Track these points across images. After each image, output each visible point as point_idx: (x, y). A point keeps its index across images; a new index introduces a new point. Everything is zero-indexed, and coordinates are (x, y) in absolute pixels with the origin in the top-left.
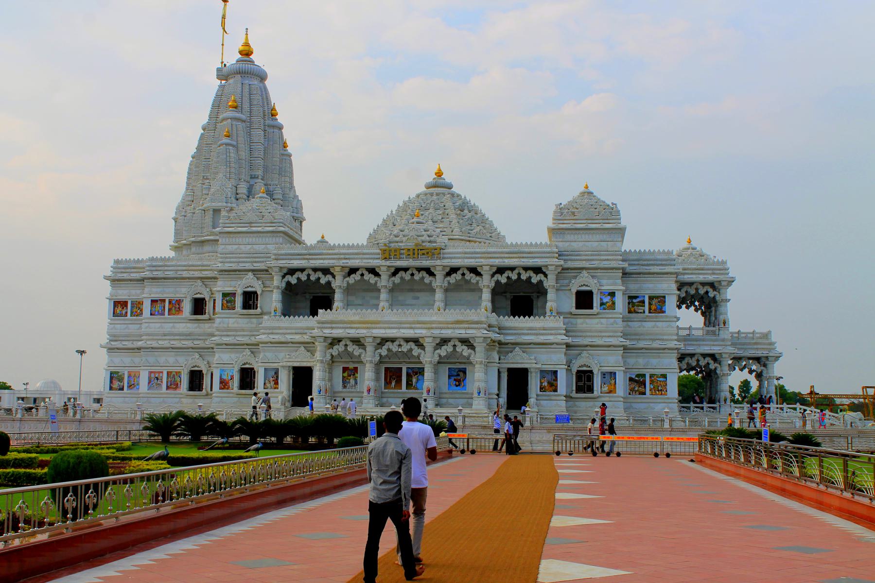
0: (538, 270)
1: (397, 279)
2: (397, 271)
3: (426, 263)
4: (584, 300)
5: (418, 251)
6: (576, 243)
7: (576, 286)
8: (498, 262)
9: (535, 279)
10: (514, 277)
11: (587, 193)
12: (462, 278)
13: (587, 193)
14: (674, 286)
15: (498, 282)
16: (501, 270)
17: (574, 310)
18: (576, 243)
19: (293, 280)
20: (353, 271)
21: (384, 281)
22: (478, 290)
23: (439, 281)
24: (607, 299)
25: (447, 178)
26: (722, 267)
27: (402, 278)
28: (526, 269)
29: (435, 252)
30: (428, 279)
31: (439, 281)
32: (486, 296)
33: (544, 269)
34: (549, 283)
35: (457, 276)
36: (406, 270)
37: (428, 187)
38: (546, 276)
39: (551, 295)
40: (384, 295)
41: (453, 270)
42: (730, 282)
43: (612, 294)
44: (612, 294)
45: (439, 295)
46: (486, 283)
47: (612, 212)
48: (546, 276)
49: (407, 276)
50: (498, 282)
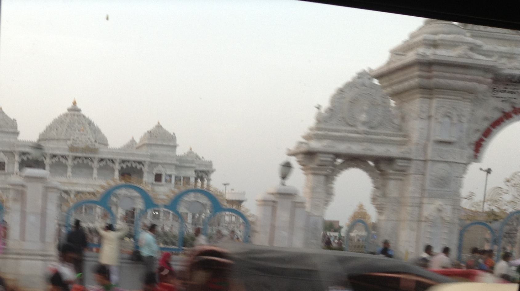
0: (140, 163)
1: (76, 162)
2: (75, 158)
3: (91, 155)
4: (158, 178)
5: (87, 149)
6: (157, 151)
7: (155, 171)
8: (124, 158)
9: (139, 167)
10: (129, 165)
11: (159, 126)
12: (106, 164)
13: (159, 126)
14: (194, 173)
15: (122, 168)
16: (123, 161)
17: (154, 182)
18: (157, 151)
19: (25, 158)
20: (54, 156)
21: (70, 162)
22: (113, 170)
23: (96, 164)
24: (168, 178)
25: (79, 106)
26: (210, 164)
27: (78, 162)
28: (135, 162)
29: (95, 151)
30: (90, 163)
31: (96, 164)
32: (117, 173)
33: (143, 163)
34: (145, 169)
35: (104, 163)
36: (79, 158)
37: (69, 110)
38: (143, 165)
39: (145, 175)
40: (69, 169)
41: (102, 160)
42: (213, 171)
43: (170, 176)
44: (170, 176)
45: (95, 171)
46: (117, 167)
47: (173, 138)
48: (143, 165)
49: (80, 161)
50: (122, 168)
